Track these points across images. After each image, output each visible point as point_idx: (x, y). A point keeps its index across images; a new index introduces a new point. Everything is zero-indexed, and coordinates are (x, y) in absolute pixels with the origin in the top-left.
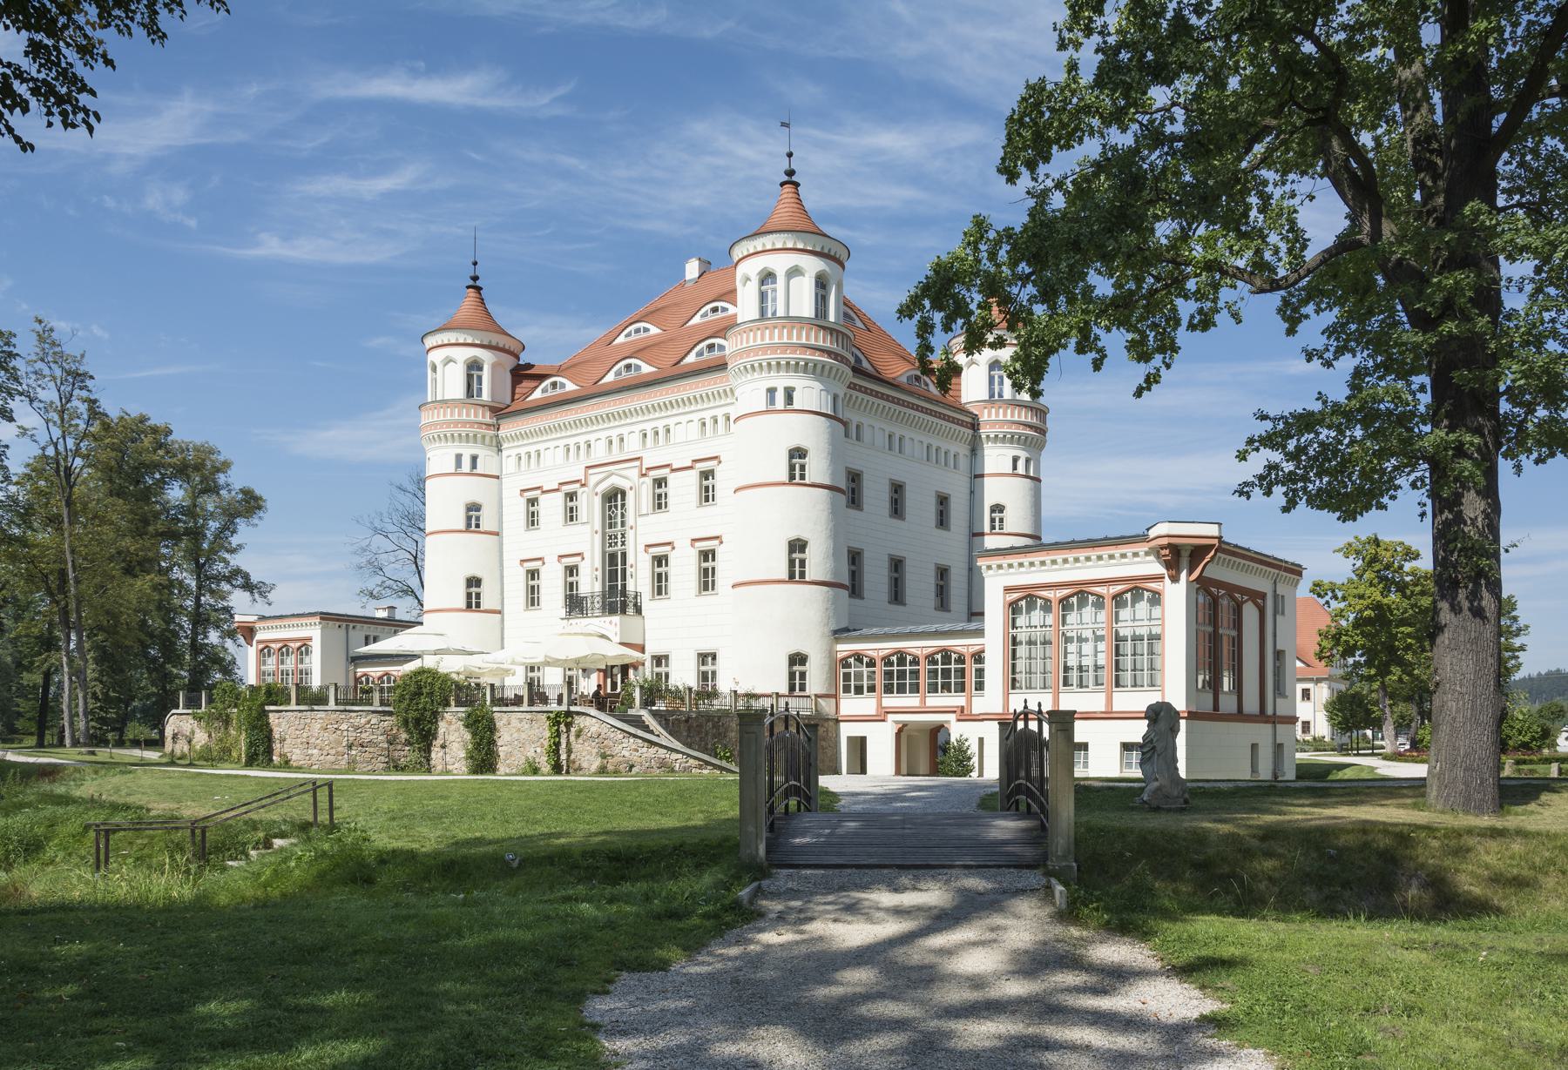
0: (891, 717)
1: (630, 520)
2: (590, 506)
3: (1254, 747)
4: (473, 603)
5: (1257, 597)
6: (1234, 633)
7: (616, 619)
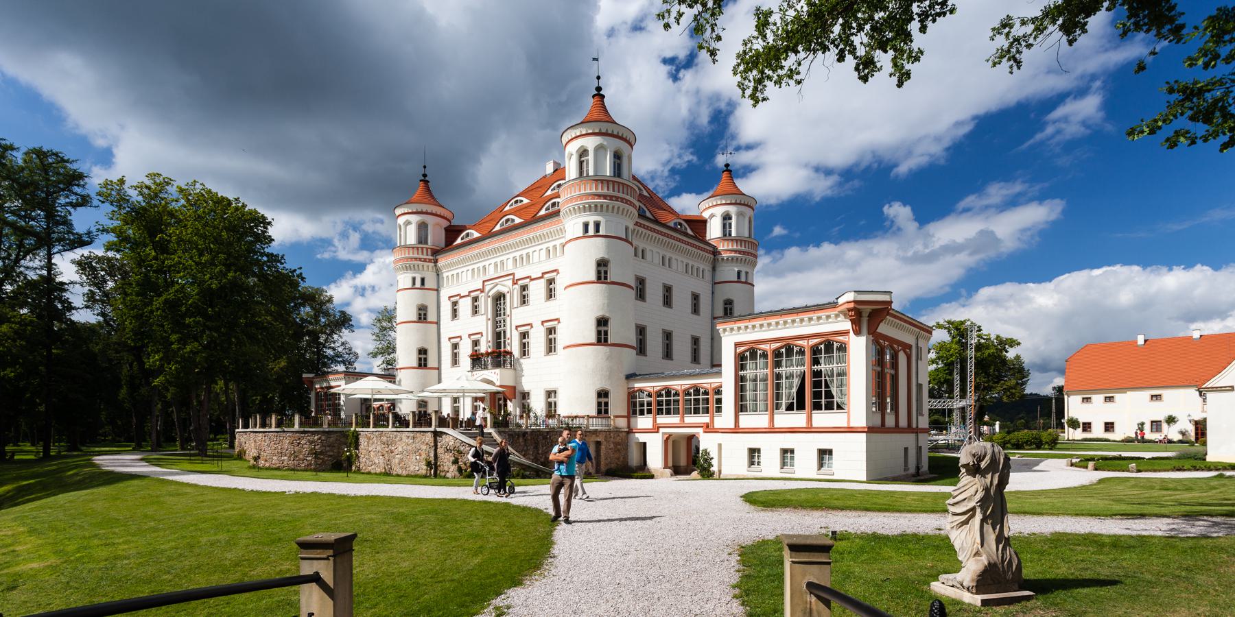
0: (662, 430)
1: (508, 312)
2: (486, 305)
3: (906, 449)
4: (422, 364)
5: (906, 347)
6: (893, 372)
7: (498, 371)
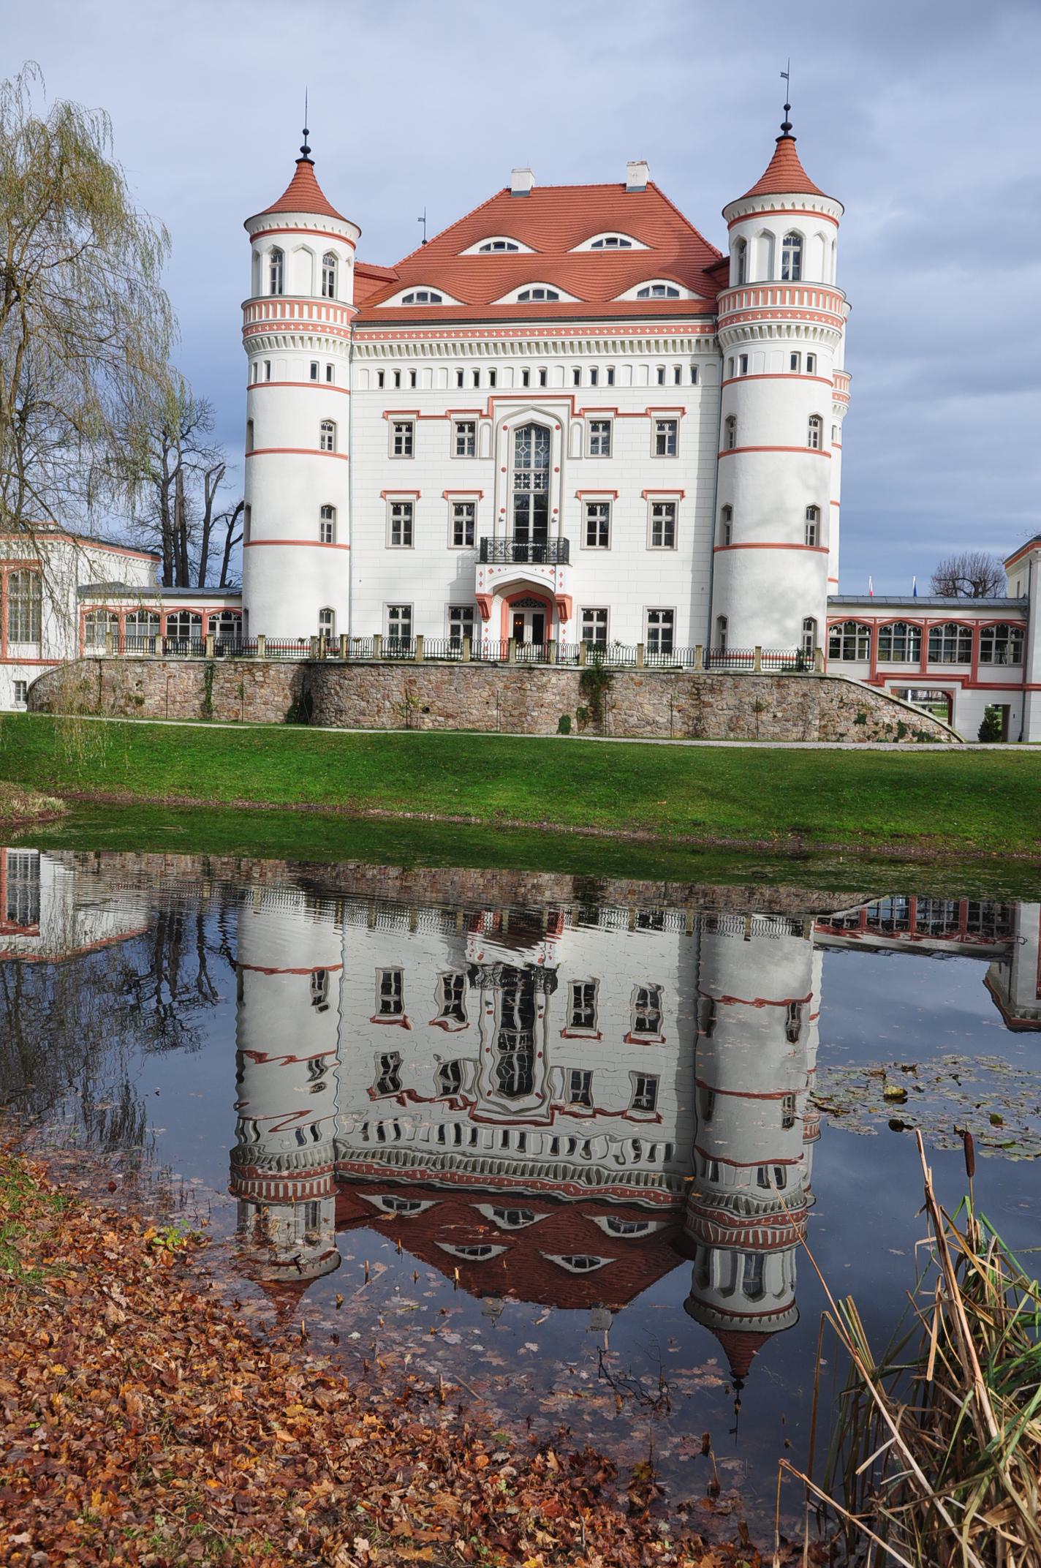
1: (555, 462)
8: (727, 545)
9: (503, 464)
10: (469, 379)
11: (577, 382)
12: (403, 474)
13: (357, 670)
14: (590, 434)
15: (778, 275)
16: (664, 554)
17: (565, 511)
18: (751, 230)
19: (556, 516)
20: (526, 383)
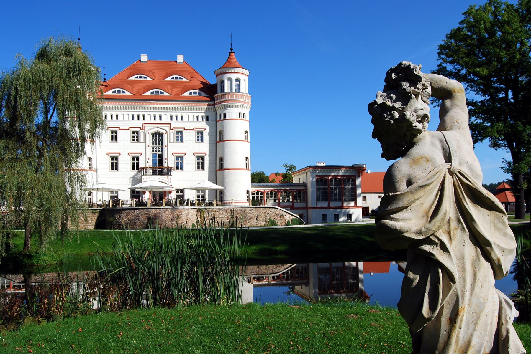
1: (165, 143)
8: (221, 168)
9: (148, 144)
10: (136, 118)
11: (171, 119)
12: (114, 147)
13: (126, 211)
14: (176, 135)
15: (234, 91)
16: (200, 172)
17: (169, 159)
18: (226, 77)
19: (166, 161)
20: (155, 119)
